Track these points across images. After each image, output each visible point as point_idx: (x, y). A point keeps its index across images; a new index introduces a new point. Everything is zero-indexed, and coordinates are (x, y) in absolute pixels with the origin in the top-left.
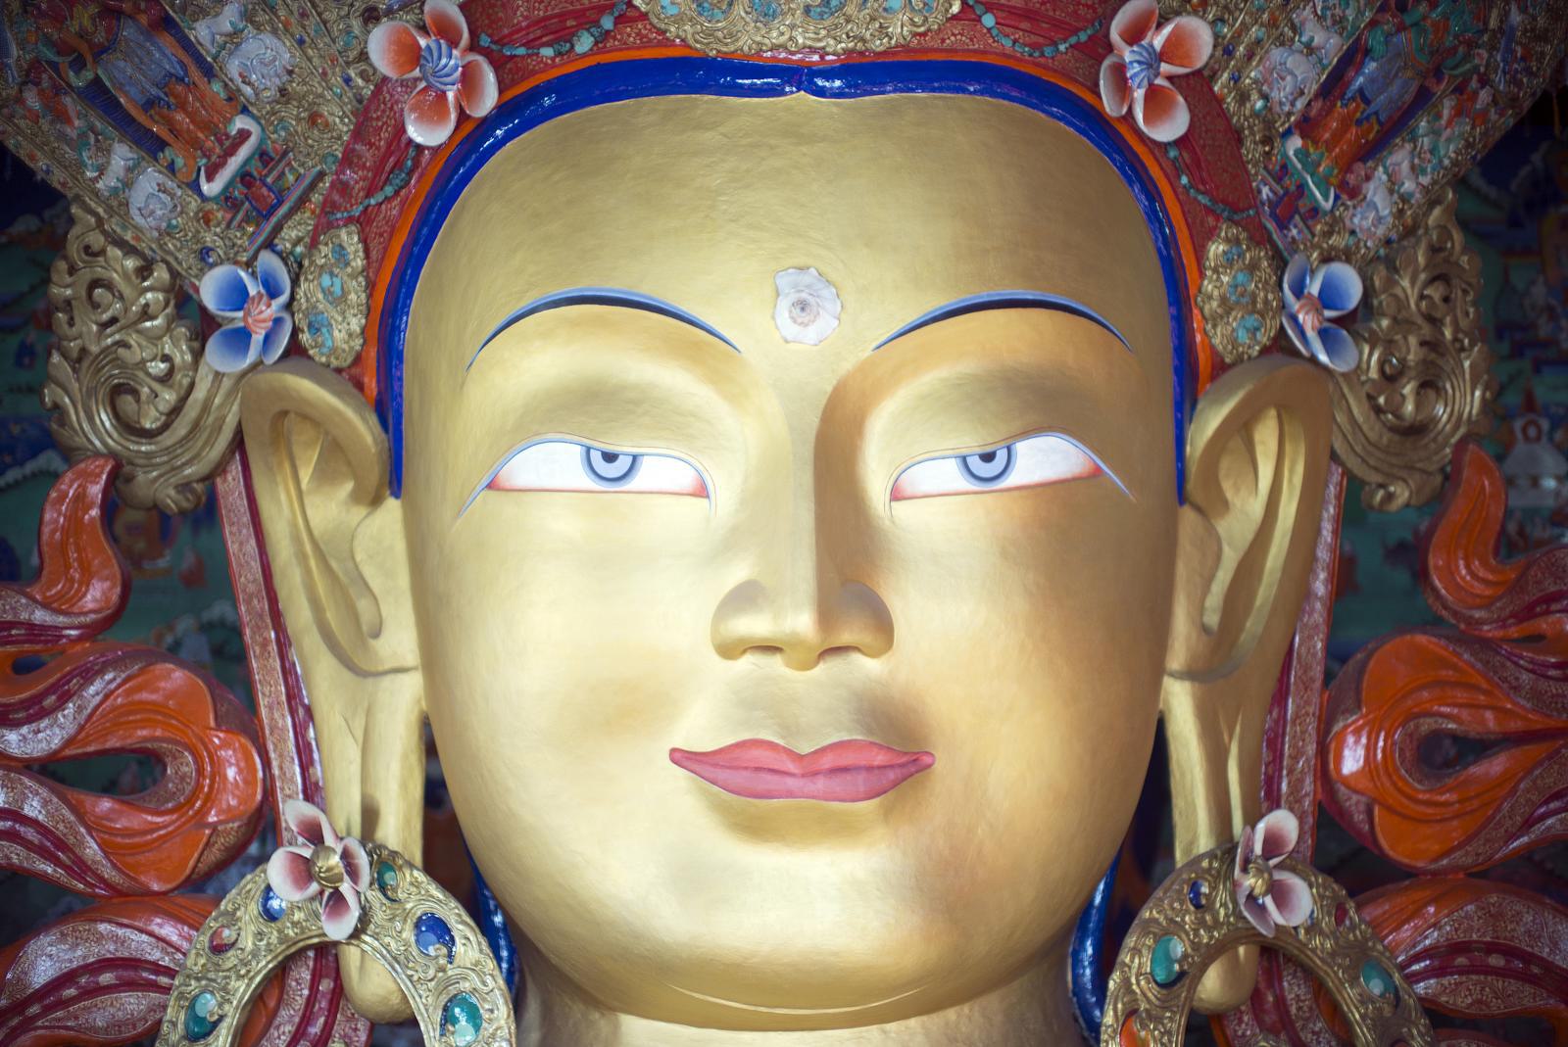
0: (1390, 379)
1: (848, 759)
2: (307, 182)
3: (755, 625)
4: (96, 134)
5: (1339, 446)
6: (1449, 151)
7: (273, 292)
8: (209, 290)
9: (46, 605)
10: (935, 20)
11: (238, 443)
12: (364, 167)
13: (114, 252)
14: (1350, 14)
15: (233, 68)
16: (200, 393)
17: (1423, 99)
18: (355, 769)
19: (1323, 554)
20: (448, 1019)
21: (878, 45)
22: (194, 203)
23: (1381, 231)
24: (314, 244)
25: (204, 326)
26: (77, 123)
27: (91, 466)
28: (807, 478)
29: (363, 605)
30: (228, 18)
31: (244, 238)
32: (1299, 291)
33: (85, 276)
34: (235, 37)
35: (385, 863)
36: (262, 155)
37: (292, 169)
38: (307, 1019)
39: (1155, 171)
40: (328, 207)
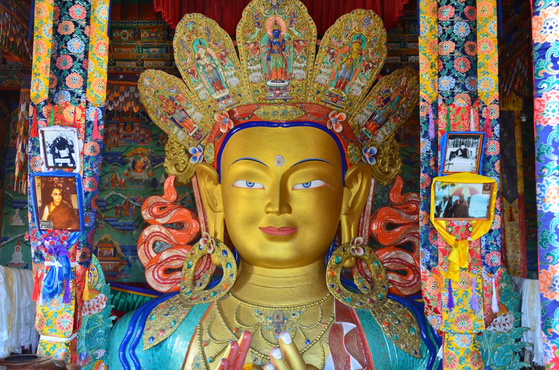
0: (383, 164)
1: (285, 229)
3: (270, 209)
5: (374, 176)
6: (393, 127)
7: (201, 151)
8: (190, 151)
9: (165, 199)
10: (300, 115)
11: (195, 173)
13: (176, 143)
14: (373, 108)
15: (194, 117)
16: (189, 166)
17: (387, 119)
18: (213, 226)
19: (371, 193)
20: (227, 266)
21: (291, 120)
22: (188, 137)
23: (381, 141)
24: (206, 145)
25: (190, 156)
27: (172, 177)
28: (278, 188)
29: (215, 201)
30: (193, 110)
31: (196, 142)
32: (365, 151)
33: (171, 147)
35: (217, 242)
36: (199, 131)
38: (206, 265)
39: (338, 135)
40: (209, 140)
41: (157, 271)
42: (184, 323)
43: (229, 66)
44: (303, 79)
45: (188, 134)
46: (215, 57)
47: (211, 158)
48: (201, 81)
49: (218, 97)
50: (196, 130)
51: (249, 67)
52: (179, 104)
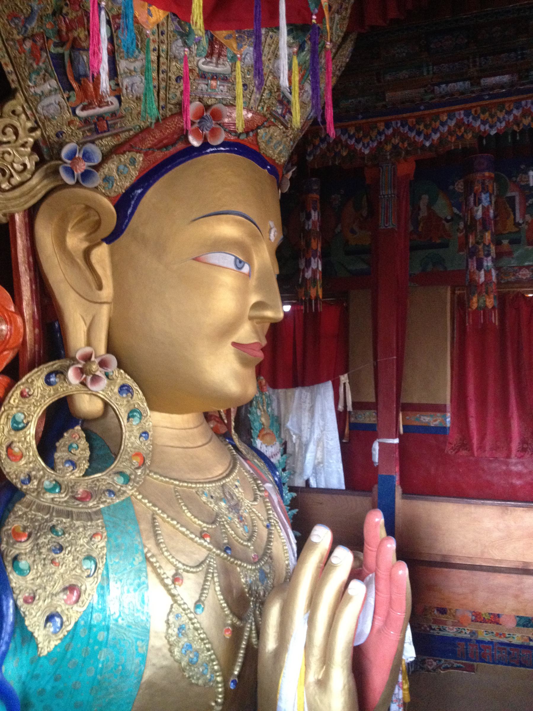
2: (123, 129)
4: (46, 71)
12: (154, 137)
13: (23, 116)
22: (68, 115)
26: (41, 64)
33: (7, 121)
34: (130, 73)
36: (113, 114)
37: (121, 123)
49: (205, 68)
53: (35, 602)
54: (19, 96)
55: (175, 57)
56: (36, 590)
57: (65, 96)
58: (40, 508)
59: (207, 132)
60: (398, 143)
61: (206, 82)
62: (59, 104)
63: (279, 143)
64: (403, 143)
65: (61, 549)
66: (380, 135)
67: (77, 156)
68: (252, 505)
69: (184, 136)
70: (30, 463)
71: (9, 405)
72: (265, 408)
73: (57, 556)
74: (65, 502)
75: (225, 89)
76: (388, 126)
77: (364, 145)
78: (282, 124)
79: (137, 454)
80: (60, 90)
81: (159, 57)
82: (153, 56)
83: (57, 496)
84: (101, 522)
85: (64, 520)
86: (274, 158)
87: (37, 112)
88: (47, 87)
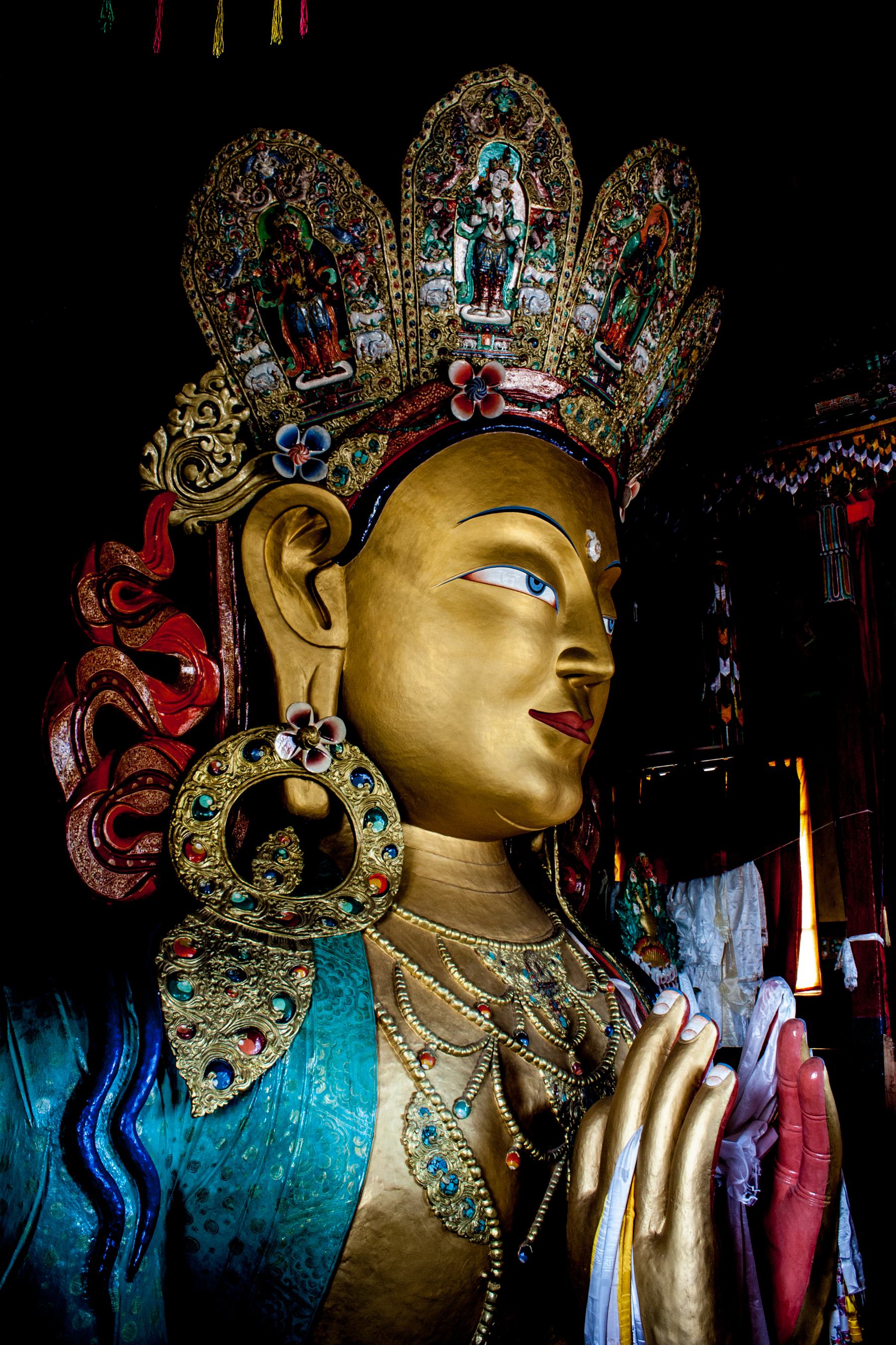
4: (255, 332)
13: (226, 392)
22: (284, 389)
26: (248, 323)
33: (205, 396)
34: (366, 329)
36: (346, 383)
37: (357, 397)
41: (100, 823)
42: (319, 1004)
43: (545, 256)
44: (640, 375)
45: (293, 381)
46: (519, 215)
47: (358, 480)
48: (451, 254)
49: (473, 318)
50: (335, 378)
51: (587, 286)
52: (333, 280)
53: (194, 1039)
54: (222, 368)
55: (427, 304)
56: (199, 1024)
57: (281, 364)
58: (220, 924)
59: (479, 401)
60: (842, 473)
61: (475, 337)
62: (273, 374)
63: (596, 422)
64: (849, 473)
65: (241, 976)
66: (814, 465)
67: (298, 443)
68: (579, 995)
69: (444, 407)
70: (216, 866)
71: (193, 783)
72: (648, 903)
73: (235, 984)
74: (259, 922)
75: (504, 346)
76: (823, 450)
77: (788, 482)
78: (603, 398)
79: (378, 876)
80: (274, 355)
81: (404, 305)
82: (397, 305)
83: (249, 912)
84: (309, 954)
85: (254, 943)
86: (591, 444)
87: (245, 386)
88: (256, 352)
